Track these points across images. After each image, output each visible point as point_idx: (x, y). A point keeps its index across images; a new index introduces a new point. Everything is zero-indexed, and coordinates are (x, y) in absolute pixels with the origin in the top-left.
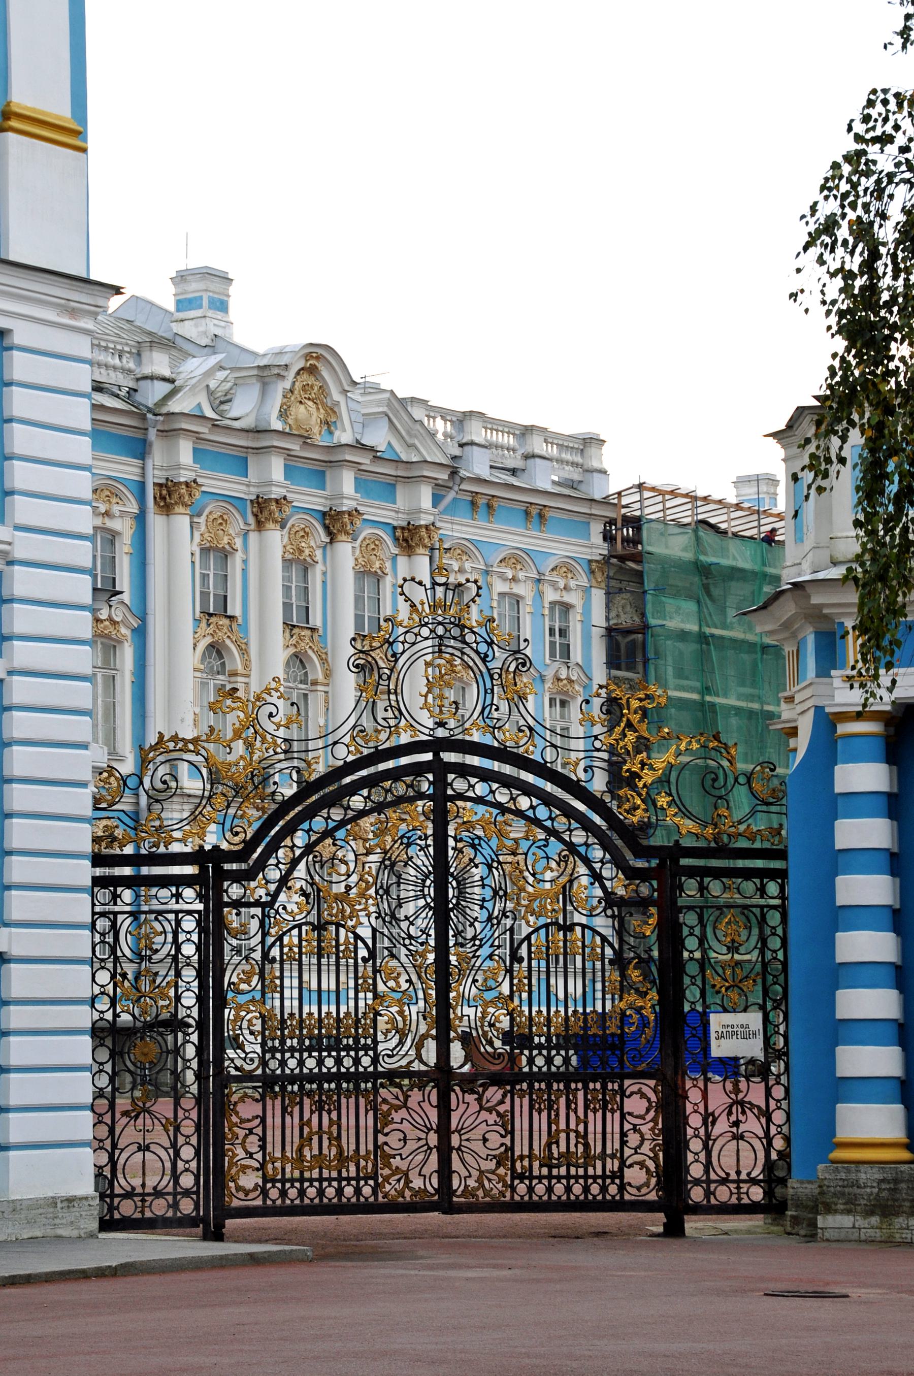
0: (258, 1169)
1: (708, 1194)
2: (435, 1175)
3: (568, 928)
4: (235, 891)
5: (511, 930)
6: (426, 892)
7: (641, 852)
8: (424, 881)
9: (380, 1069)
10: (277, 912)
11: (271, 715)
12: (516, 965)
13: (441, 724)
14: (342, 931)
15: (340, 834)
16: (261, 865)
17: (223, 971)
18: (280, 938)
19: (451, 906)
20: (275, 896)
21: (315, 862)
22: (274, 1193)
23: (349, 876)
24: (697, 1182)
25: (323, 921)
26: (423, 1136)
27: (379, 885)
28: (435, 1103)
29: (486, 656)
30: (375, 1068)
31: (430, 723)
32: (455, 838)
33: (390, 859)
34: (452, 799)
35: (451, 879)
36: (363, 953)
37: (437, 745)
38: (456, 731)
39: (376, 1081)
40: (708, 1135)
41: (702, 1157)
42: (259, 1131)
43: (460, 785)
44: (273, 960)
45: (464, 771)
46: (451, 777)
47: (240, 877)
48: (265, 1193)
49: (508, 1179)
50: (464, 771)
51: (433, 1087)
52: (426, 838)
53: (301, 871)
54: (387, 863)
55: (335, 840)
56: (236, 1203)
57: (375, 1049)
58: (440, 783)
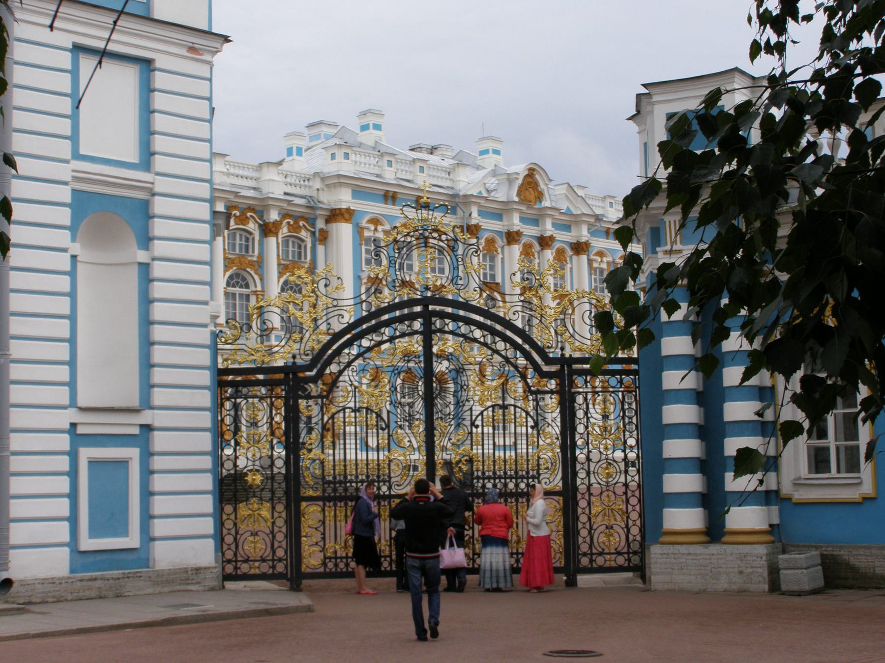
1: (591, 561)
3: (504, 407)
5: (471, 409)
7: (549, 361)
11: (326, 286)
12: (474, 430)
18: (332, 417)
24: (585, 554)
29: (454, 248)
34: (435, 332)
37: (425, 302)
40: (591, 528)
41: (588, 539)
43: (438, 324)
45: (442, 315)
49: (471, 555)
50: (442, 315)
57: (389, 481)
58: (427, 324)
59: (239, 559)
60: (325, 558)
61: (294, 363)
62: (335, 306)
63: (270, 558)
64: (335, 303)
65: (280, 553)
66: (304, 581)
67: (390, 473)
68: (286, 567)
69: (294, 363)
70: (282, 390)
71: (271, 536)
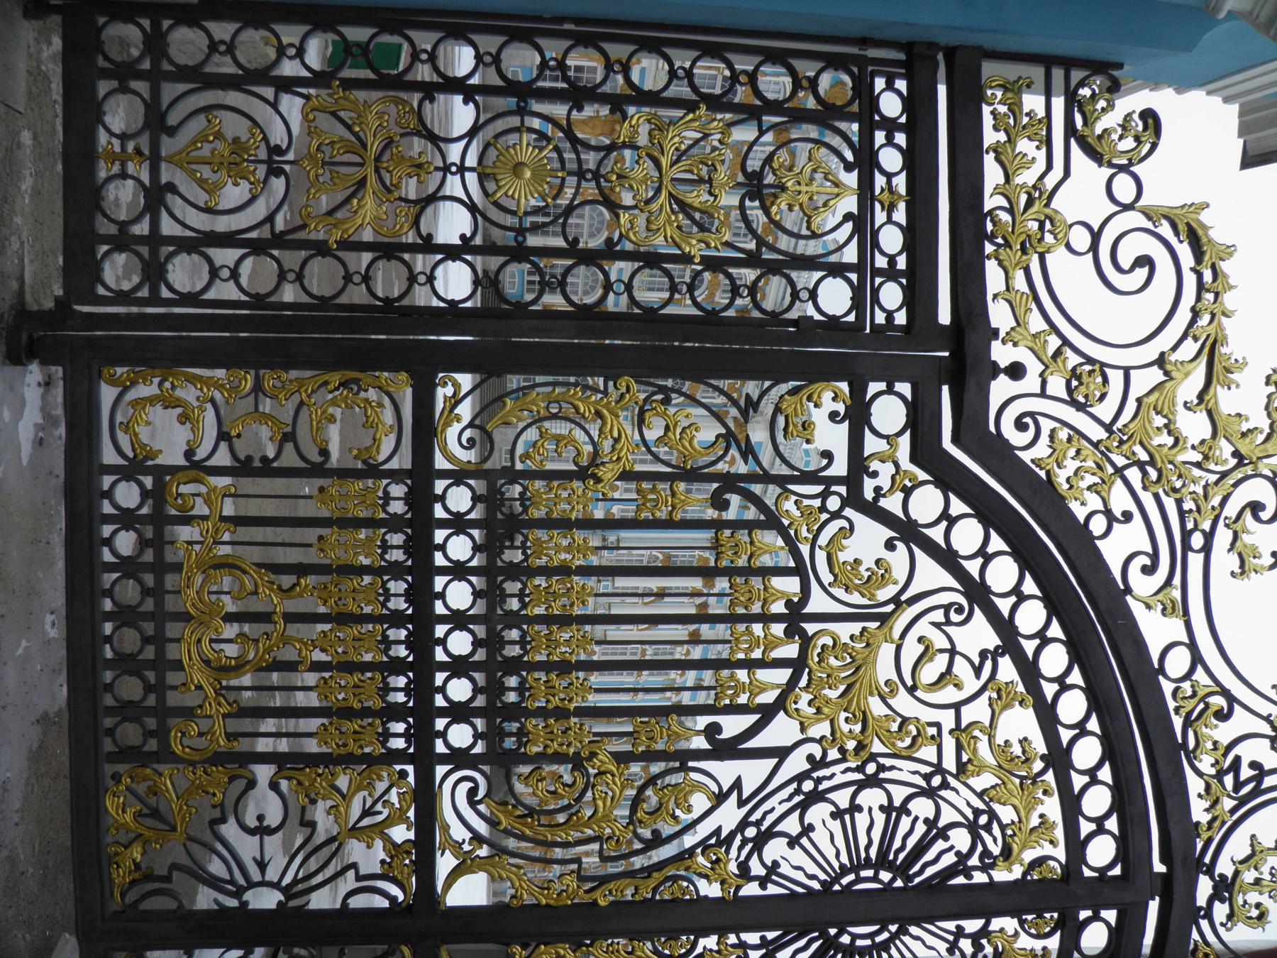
0: (189, 454)
2: (173, 905)
4: (889, 413)
6: (864, 874)
8: (890, 866)
9: (441, 770)
10: (836, 515)
11: (1255, 507)
13: (1224, 888)
14: (783, 675)
15: (1007, 670)
16: (949, 478)
17: (699, 379)
19: (833, 931)
20: (875, 512)
21: (947, 608)
22: (128, 495)
23: (912, 690)
25: (811, 628)
26: (272, 875)
27: (888, 762)
28: (358, 902)
30: (443, 759)
31: (1224, 867)
32: (984, 932)
33: (945, 785)
35: (893, 928)
36: (732, 725)
38: (1204, 924)
39: (410, 759)
42: (290, 459)
44: (719, 502)
46: (1111, 915)
47: (920, 421)
48: (130, 471)
51: (393, 899)
52: (984, 868)
53: (931, 574)
54: (936, 781)
55: (996, 654)
56: (108, 394)
59: (170, 91)
60: (160, 472)
61: (995, 370)
62: (1186, 535)
63: (168, 227)
64: (1197, 540)
65: (184, 273)
66: (60, 369)
67: (526, 759)
68: (122, 297)
69: (995, 370)
70: (890, 315)
71: (265, 232)
